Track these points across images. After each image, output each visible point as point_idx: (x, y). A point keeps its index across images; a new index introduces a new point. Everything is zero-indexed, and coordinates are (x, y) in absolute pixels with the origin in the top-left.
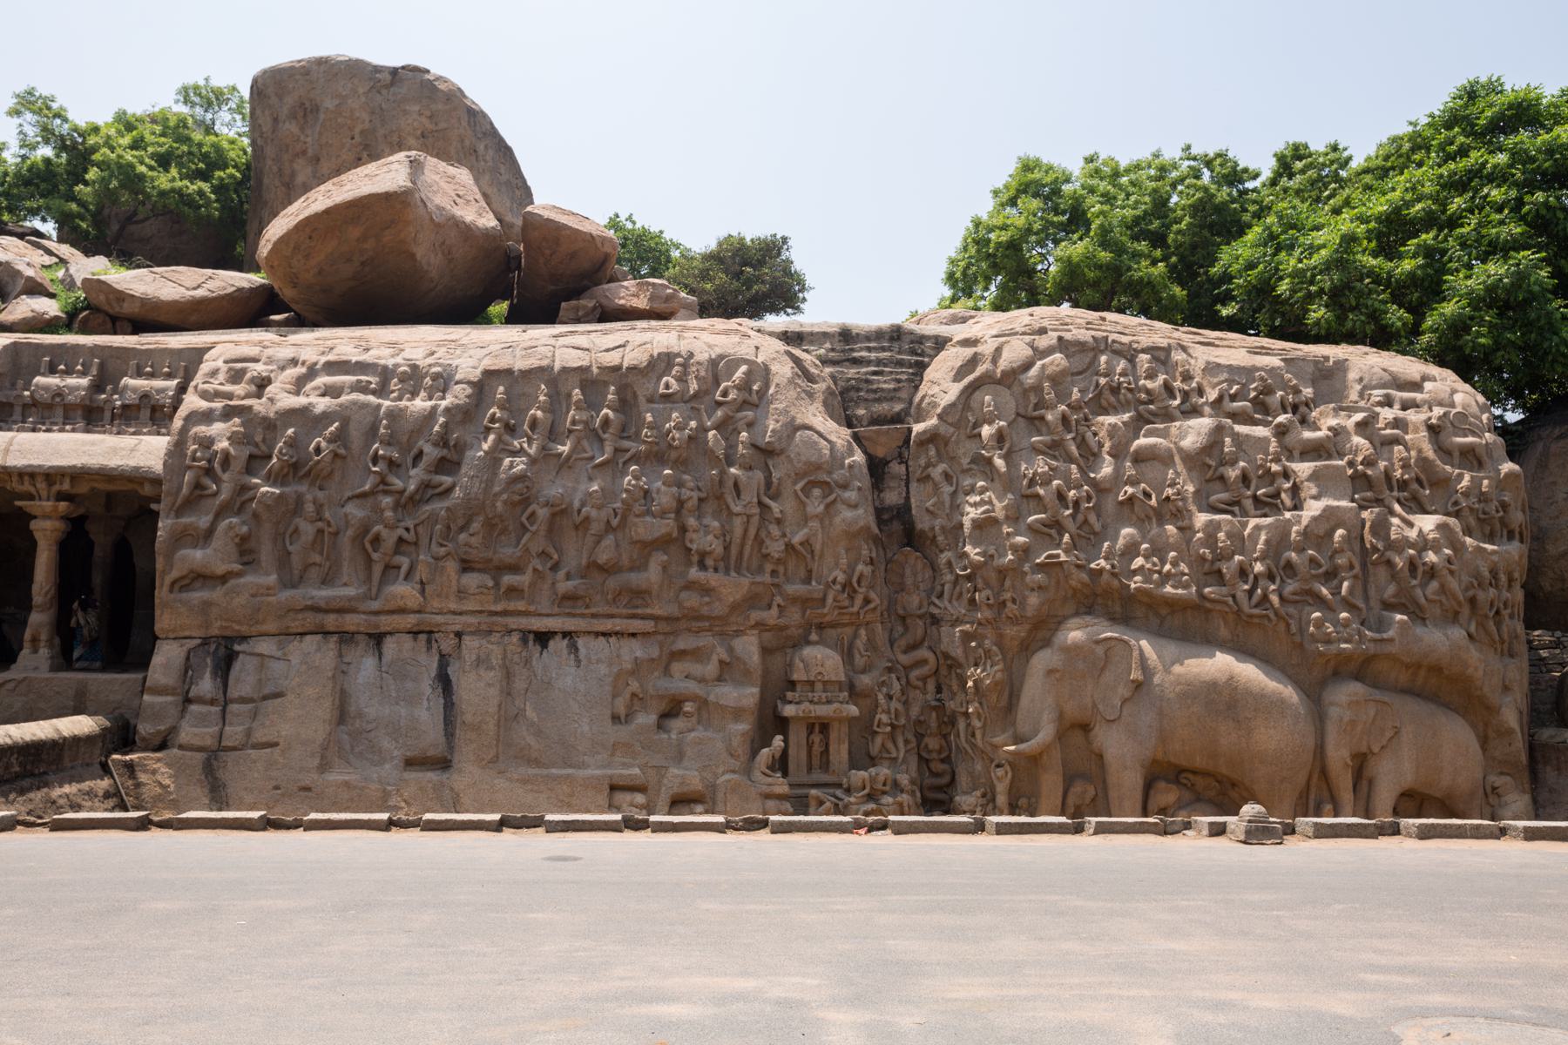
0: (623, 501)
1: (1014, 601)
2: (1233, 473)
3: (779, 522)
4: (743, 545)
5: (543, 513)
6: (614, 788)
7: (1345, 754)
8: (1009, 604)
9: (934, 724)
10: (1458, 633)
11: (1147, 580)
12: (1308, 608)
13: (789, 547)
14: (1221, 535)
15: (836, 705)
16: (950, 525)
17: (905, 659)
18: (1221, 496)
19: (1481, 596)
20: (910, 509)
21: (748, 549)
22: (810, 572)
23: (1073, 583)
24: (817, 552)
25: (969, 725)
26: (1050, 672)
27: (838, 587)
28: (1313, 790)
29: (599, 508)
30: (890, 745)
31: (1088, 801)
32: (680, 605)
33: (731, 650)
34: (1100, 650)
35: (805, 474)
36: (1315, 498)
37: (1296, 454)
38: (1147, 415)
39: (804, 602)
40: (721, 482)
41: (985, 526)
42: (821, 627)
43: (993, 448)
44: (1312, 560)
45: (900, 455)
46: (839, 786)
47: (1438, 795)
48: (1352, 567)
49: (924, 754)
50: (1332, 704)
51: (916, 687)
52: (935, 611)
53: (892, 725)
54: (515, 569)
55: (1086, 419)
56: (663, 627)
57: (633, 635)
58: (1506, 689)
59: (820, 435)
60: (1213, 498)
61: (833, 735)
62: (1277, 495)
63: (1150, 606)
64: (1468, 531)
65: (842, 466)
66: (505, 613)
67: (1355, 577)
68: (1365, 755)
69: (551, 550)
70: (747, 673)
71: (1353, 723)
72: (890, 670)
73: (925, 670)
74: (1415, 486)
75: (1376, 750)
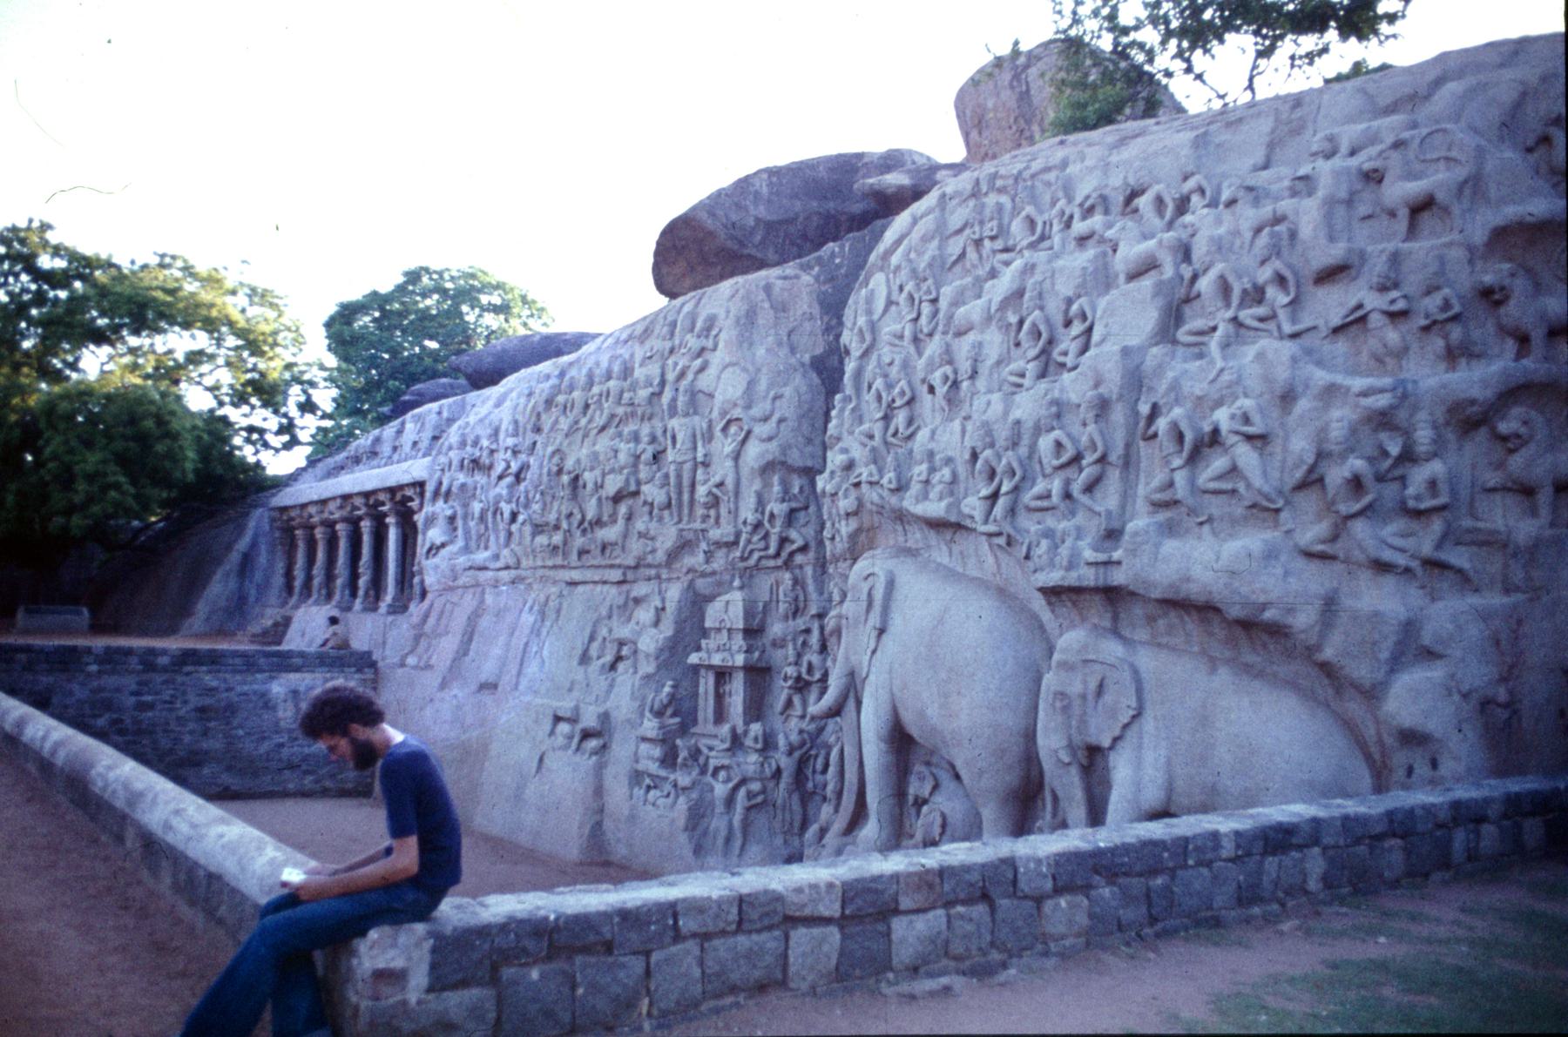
4: (680, 493)
5: (565, 479)
6: (558, 719)
19: (1336, 475)
21: (686, 497)
27: (749, 528)
36: (1099, 344)
37: (1122, 278)
46: (716, 736)
54: (557, 527)
56: (630, 576)
58: (1430, 654)
66: (555, 567)
69: (576, 511)
71: (1061, 695)
75: (1106, 743)
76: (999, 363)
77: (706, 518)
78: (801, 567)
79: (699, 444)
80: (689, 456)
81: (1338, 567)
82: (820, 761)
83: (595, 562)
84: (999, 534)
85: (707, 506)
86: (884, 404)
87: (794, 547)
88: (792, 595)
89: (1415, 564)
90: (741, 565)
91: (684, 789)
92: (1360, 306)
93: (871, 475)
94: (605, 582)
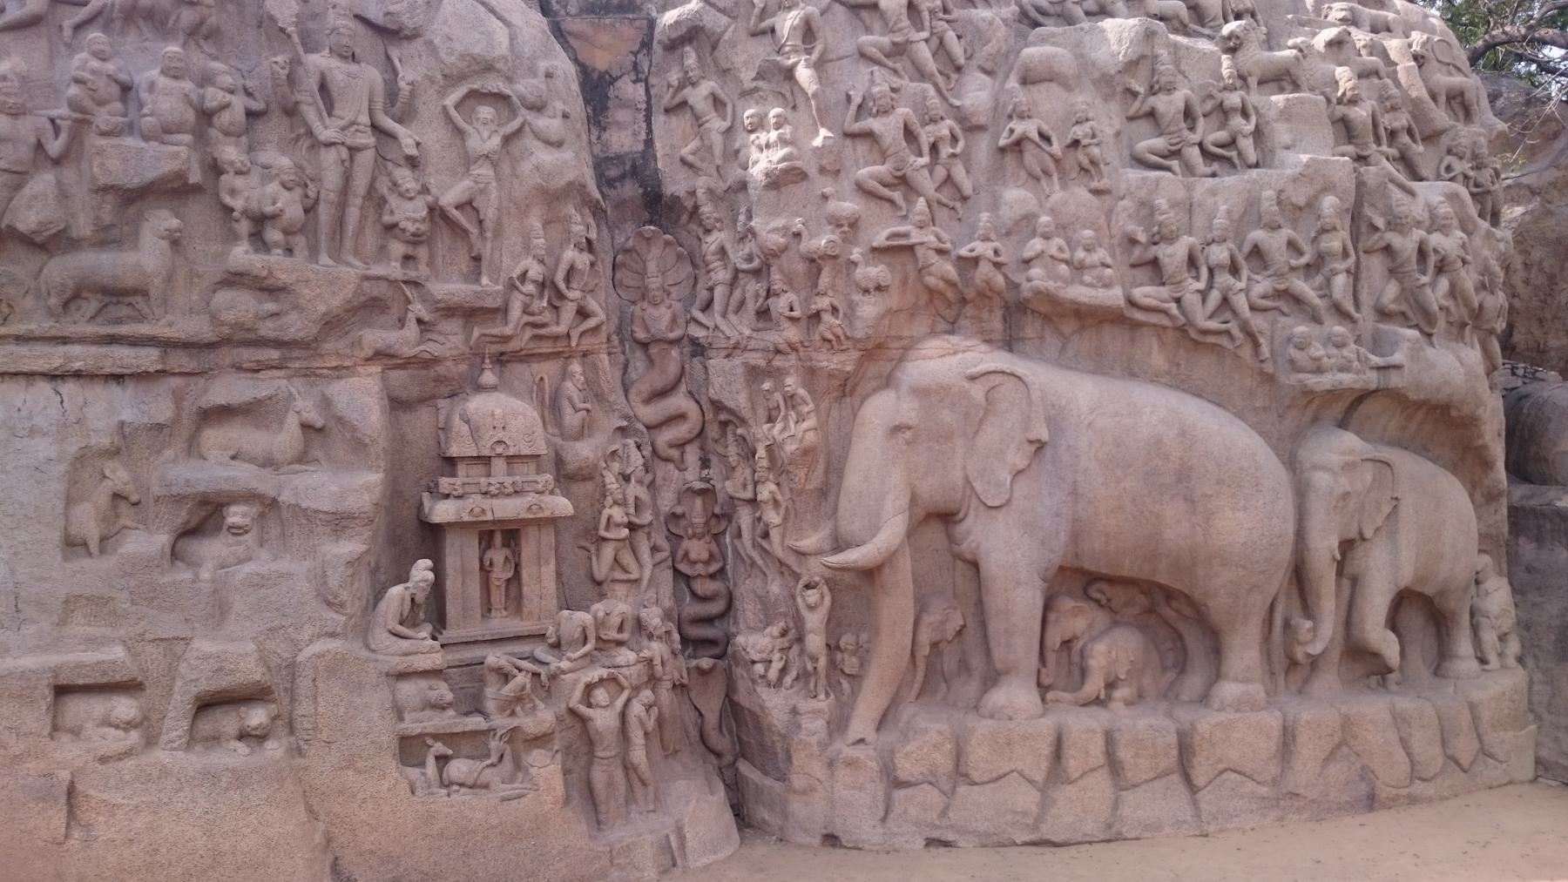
0: (74, 105)
1: (835, 310)
2: (1170, 105)
3: (413, 163)
6: (62, 691)
9: (698, 519)
12: (1283, 319)
13: (436, 213)
14: (1162, 202)
15: (530, 498)
16: (721, 187)
17: (649, 413)
18: (1151, 143)
21: (353, 214)
22: (477, 259)
23: (931, 281)
24: (489, 224)
25: (759, 519)
26: (897, 429)
27: (530, 288)
29: (15, 115)
30: (627, 559)
31: (950, 634)
32: (214, 319)
33: (326, 403)
34: (977, 392)
35: (462, 77)
36: (1287, 148)
38: (1033, 14)
39: (471, 314)
40: (291, 80)
41: (785, 179)
42: (501, 360)
43: (795, 51)
44: (1292, 245)
45: (635, 66)
48: (1345, 255)
49: (683, 567)
50: (1316, 467)
51: (667, 460)
52: (699, 333)
53: (632, 527)
55: (946, 11)
57: (118, 378)
59: (493, 11)
61: (528, 550)
62: (1232, 143)
63: (1047, 318)
65: (532, 71)
70: (359, 445)
71: (1346, 496)
73: (680, 431)
74: (1406, 139)
75: (1368, 533)
76: (1118, 134)
77: (407, 258)
78: (585, 355)
79: (388, 123)
80: (371, 141)
82: (676, 636)
83: (39, 324)
85: (416, 240)
86: (926, 149)
87: (592, 323)
90: (495, 348)
91: (541, 740)
94: (53, 377)
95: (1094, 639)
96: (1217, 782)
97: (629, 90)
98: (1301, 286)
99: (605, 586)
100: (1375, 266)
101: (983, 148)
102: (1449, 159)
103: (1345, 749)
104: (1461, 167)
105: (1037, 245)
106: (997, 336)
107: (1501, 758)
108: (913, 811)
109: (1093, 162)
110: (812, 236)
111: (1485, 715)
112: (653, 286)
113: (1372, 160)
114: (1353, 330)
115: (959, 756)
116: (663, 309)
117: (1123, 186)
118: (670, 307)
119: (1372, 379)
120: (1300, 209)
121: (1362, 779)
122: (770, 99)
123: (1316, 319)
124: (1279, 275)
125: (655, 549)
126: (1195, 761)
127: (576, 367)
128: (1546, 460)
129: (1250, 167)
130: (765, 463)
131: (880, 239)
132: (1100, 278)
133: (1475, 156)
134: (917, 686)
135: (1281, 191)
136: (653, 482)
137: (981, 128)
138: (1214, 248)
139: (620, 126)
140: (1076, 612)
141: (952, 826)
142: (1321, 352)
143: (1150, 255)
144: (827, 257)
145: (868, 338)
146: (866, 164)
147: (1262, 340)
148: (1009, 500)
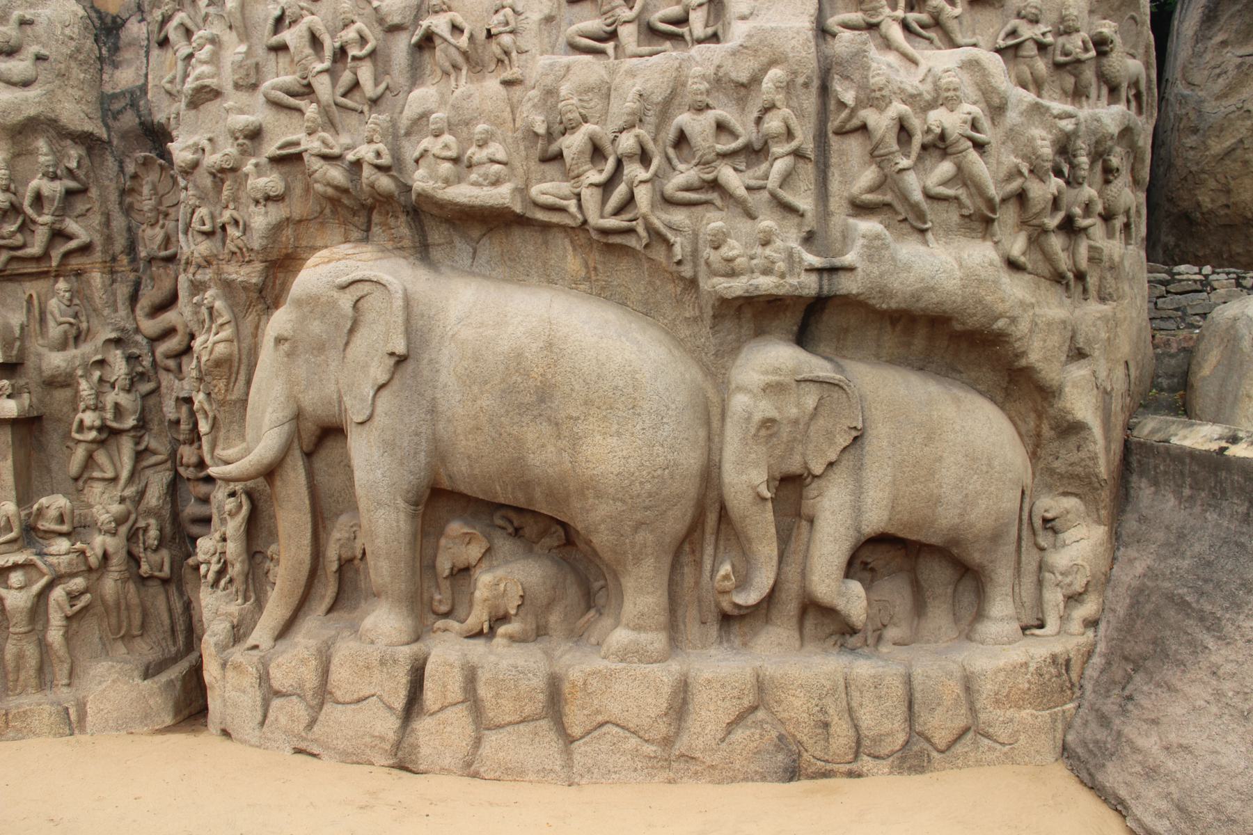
7: (758, 477)
8: (232, 232)
9: (184, 427)
10: (980, 254)
11: (433, 175)
12: (711, 213)
14: (564, 90)
17: (150, 326)
20: (146, 93)
26: (279, 340)
28: (710, 538)
34: (345, 301)
44: (721, 127)
47: (934, 540)
49: (181, 470)
50: (740, 389)
51: (168, 370)
58: (1078, 354)
60: (574, 28)
62: (682, 21)
64: (1038, 85)
67: (798, 154)
68: (801, 476)
71: (768, 423)
72: (117, 342)
75: (818, 469)
76: (549, 19)
78: (79, 274)
81: (1027, 277)
82: (153, 533)
84: (630, 231)
86: (328, 53)
87: (73, 244)
88: (71, 311)
89: (1070, 275)
92: (1013, 33)
93: (324, 142)
95: (491, 568)
96: (596, 733)
97: (135, 30)
98: (728, 175)
99: (80, 483)
100: (854, 147)
101: (401, 45)
102: (1014, 22)
103: (761, 714)
104: (1027, 32)
105: (426, 142)
106: (407, 243)
107: (1003, 738)
108: (283, 720)
109: (507, 53)
110: (214, 152)
111: (987, 688)
112: (146, 208)
113: (883, 27)
114: (800, 226)
115: (325, 673)
116: (157, 229)
117: (534, 74)
118: (163, 227)
119: (809, 285)
120: (743, 85)
121: (778, 749)
122: (216, 22)
123: (751, 216)
124: (704, 164)
125: (139, 455)
126: (567, 709)
127: (62, 285)
128: (1192, 386)
129: (700, 41)
130: (194, 374)
131: (271, 148)
132: (486, 177)
133: (1063, 19)
134: (327, 602)
135: (719, 67)
136: (156, 391)
137: (395, 29)
138: (624, 136)
139: (129, 63)
140: (469, 539)
141: (315, 741)
142: (735, 252)
143: (554, 148)
144: (222, 170)
145: (264, 248)
146: (287, 74)
147: (671, 237)
148: (370, 418)
